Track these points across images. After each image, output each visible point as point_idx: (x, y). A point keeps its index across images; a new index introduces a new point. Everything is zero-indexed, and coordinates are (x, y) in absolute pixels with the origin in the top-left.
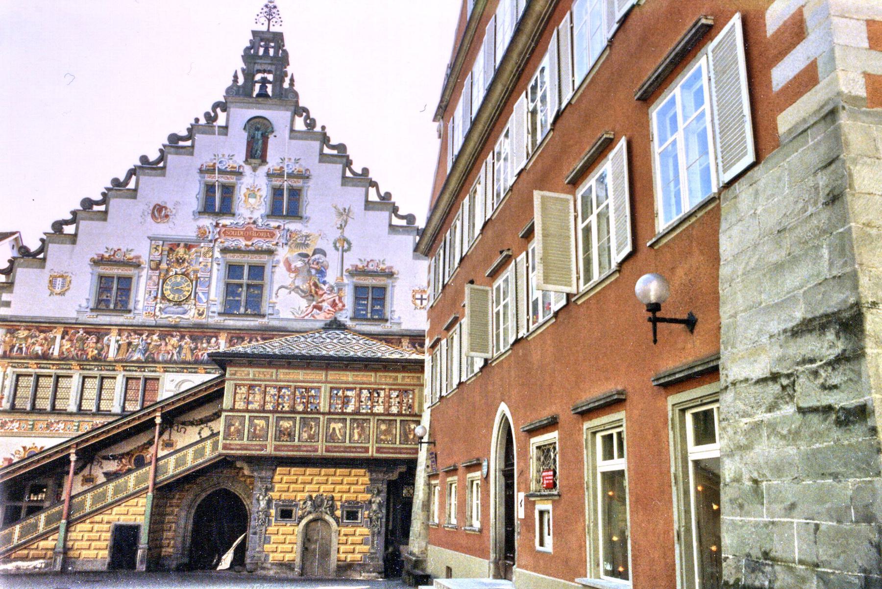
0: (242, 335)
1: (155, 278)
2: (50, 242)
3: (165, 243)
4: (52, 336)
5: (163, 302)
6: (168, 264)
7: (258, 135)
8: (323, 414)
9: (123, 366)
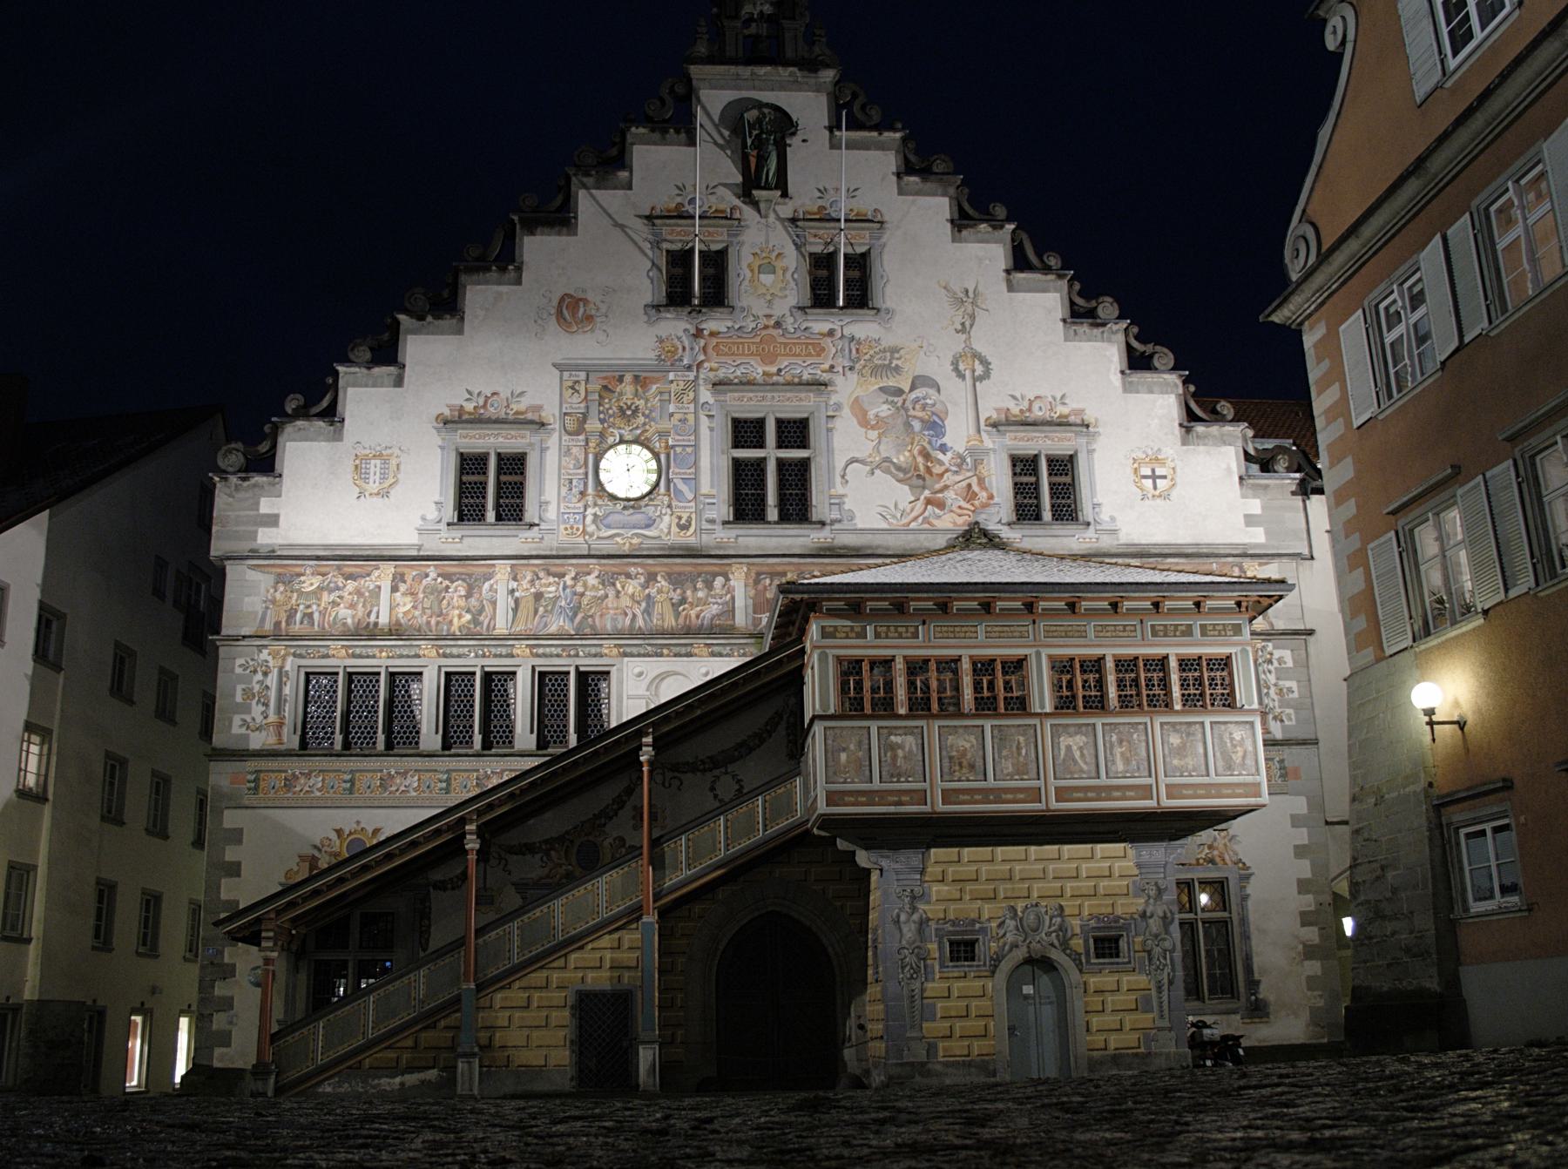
0: (780, 569)
1: (577, 452)
2: (348, 385)
4: (372, 587)
5: (600, 502)
6: (602, 421)
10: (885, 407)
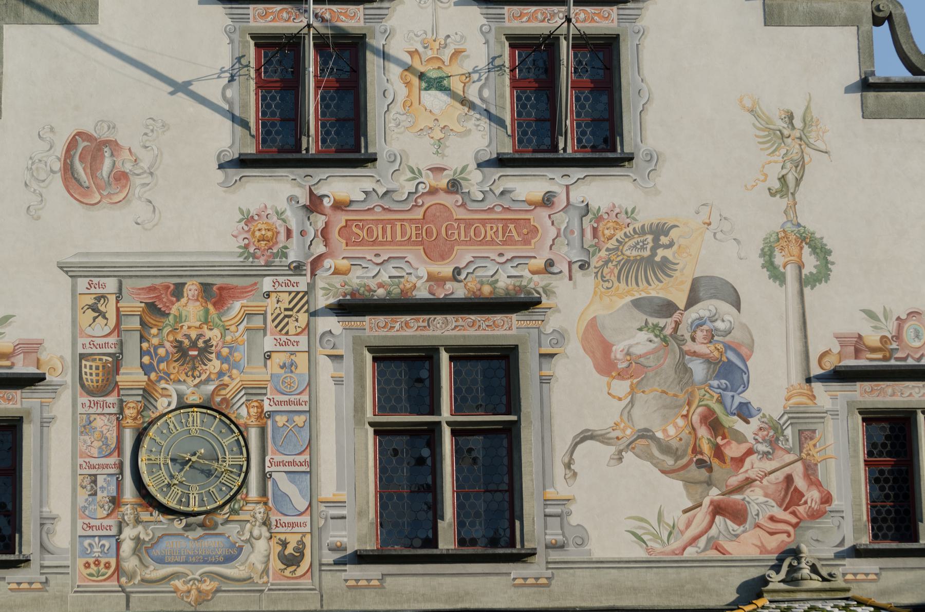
1: (105, 425)
3: (127, 283)
5: (145, 516)
10: (644, 336)
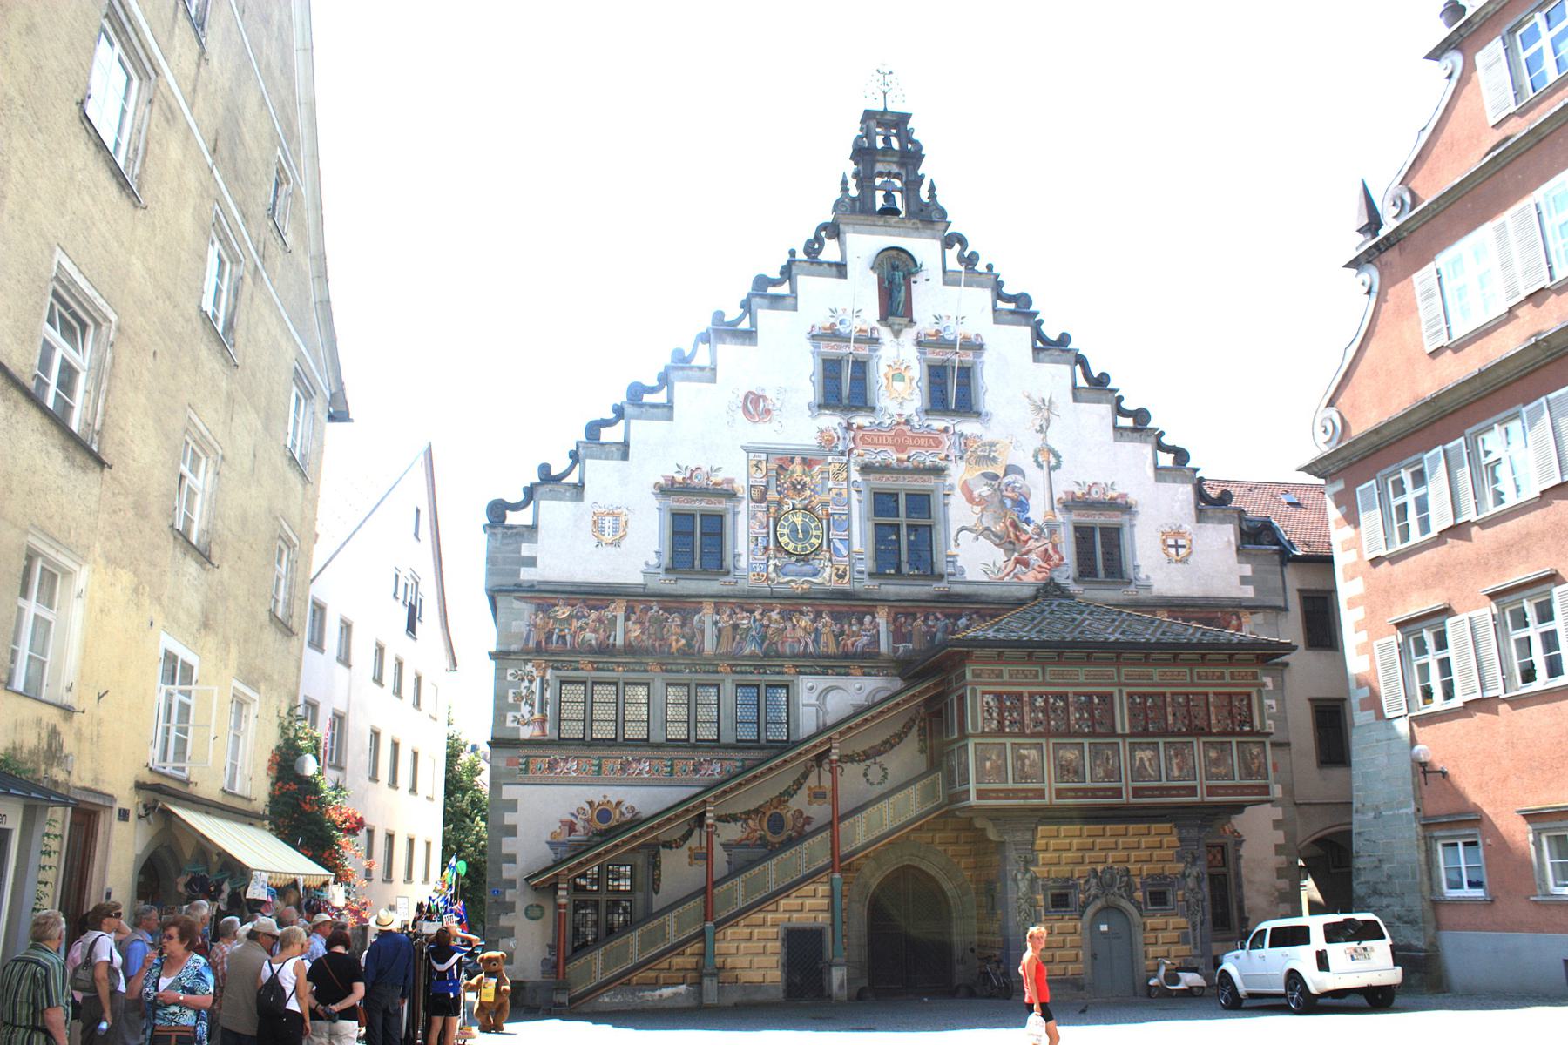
0: (912, 610)
2: (586, 457)
3: (770, 456)
4: (610, 616)
5: (779, 555)
6: (779, 493)
7: (899, 275)
8: (1123, 736)
9: (731, 666)
10: (986, 488)
